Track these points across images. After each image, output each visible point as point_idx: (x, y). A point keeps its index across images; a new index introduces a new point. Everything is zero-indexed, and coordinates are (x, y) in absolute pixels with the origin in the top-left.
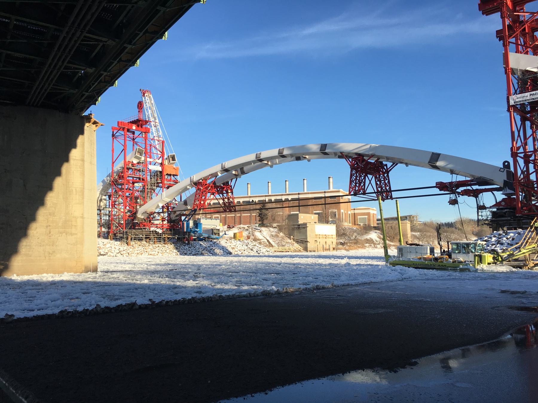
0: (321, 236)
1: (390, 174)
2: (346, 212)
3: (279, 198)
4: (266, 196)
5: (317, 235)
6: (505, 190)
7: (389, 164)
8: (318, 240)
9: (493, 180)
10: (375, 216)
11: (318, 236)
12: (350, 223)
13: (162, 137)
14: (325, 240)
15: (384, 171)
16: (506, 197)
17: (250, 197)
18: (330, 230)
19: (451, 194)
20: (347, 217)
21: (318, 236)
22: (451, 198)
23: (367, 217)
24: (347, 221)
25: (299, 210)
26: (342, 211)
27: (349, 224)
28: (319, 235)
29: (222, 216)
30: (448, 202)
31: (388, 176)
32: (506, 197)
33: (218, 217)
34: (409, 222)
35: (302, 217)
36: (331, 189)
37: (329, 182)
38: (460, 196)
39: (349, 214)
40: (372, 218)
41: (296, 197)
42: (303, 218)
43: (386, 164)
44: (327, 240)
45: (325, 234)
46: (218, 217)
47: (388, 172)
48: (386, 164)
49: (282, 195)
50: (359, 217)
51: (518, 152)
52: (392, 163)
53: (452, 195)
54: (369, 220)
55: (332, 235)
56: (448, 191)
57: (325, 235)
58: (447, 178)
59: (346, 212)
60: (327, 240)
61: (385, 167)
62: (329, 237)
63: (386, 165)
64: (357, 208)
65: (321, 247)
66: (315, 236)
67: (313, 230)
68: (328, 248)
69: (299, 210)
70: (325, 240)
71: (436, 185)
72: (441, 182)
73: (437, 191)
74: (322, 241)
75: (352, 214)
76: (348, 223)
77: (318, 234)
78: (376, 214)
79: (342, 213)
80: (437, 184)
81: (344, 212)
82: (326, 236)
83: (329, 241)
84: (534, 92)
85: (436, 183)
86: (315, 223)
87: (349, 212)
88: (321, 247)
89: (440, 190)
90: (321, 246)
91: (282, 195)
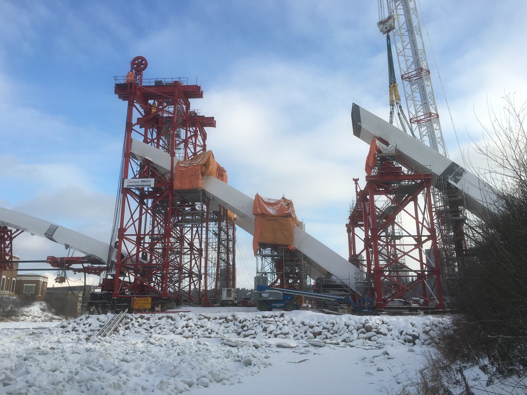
1: (14, 241)
6: (110, 272)
7: (14, 230)
9: (102, 259)
10: (45, 284)
15: (6, 236)
16: (112, 278)
19: (60, 270)
22: (59, 275)
23: (35, 285)
24: (9, 288)
26: (4, 277)
27: (11, 292)
30: (55, 280)
31: (11, 243)
32: (112, 278)
38: (77, 273)
39: (14, 281)
43: (12, 230)
47: (11, 239)
48: (12, 230)
50: (25, 285)
51: (125, 234)
52: (16, 230)
53: (61, 271)
56: (58, 267)
58: (61, 252)
59: (9, 278)
61: (9, 233)
63: (11, 231)
71: (47, 259)
72: (53, 257)
73: (49, 266)
76: (10, 291)
79: (4, 279)
80: (48, 259)
84: (145, 179)
85: (48, 257)
87: (14, 279)
89: (52, 266)
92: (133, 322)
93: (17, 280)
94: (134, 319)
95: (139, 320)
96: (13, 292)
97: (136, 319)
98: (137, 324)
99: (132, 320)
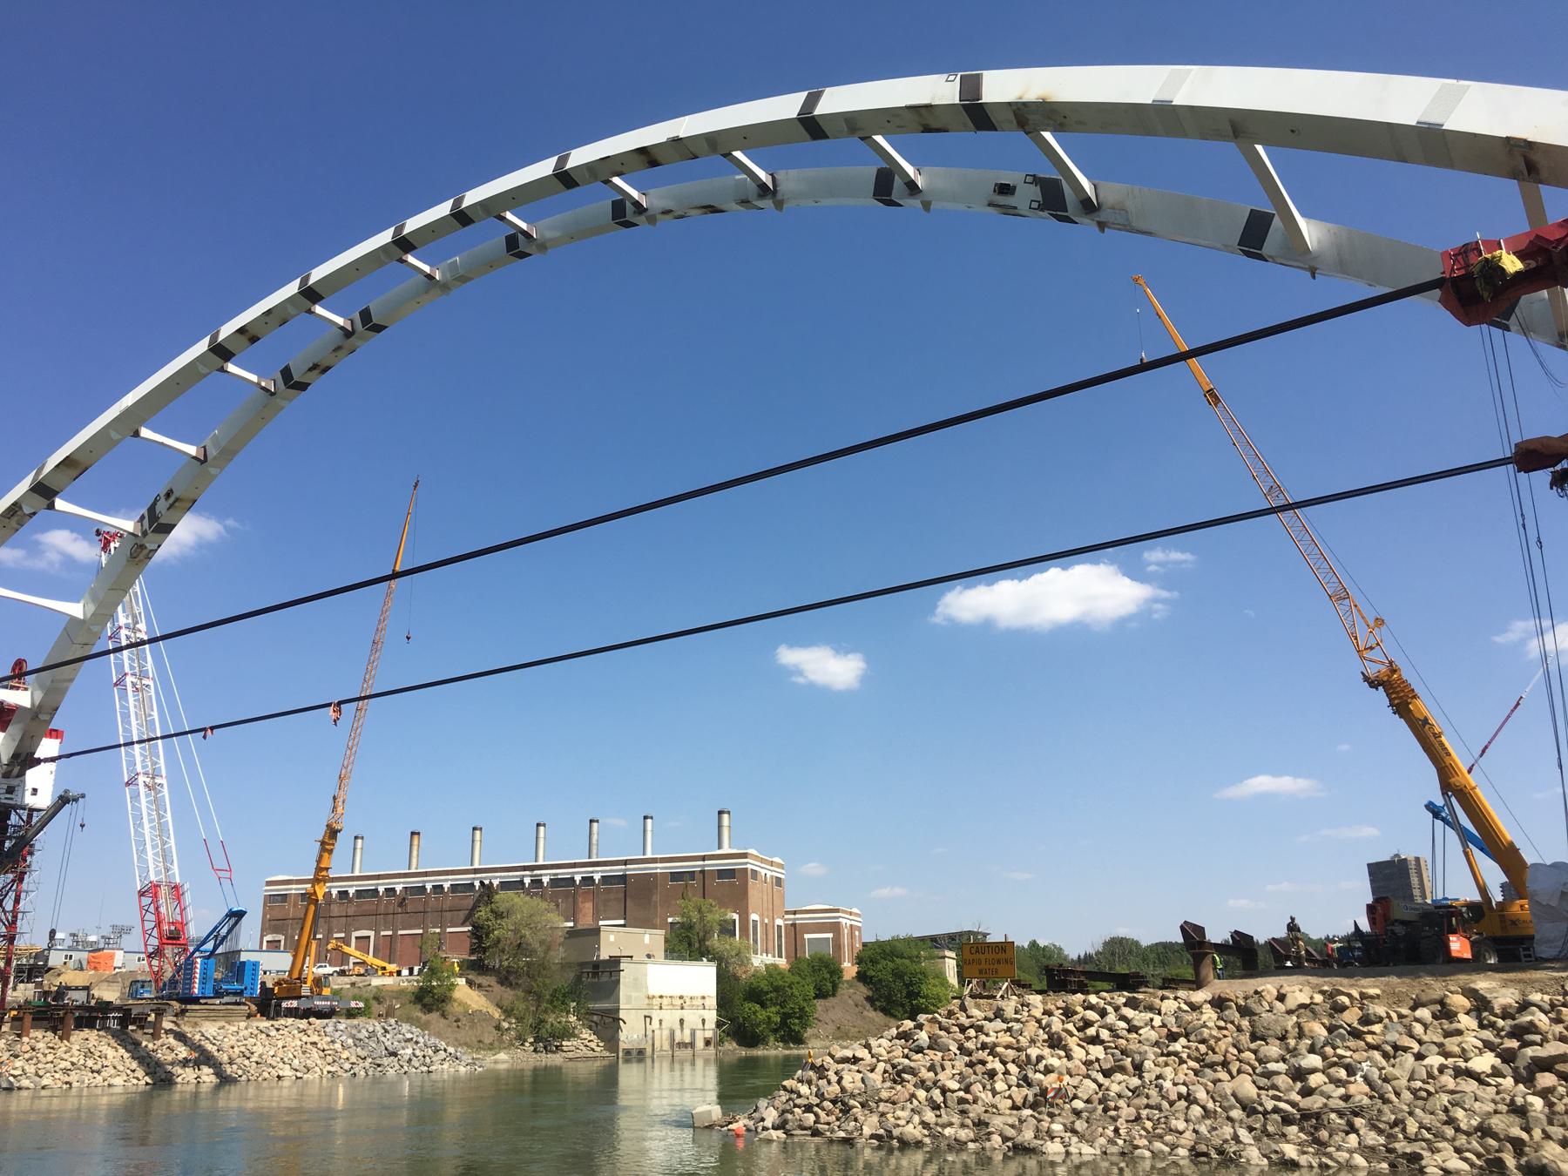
0: (665, 1002)
2: (766, 921)
3: (563, 873)
4: (525, 868)
5: (654, 997)
8: (656, 1015)
10: (857, 933)
11: (656, 1002)
12: (780, 956)
13: (151, 676)
14: (678, 1014)
17: (476, 871)
18: (700, 979)
20: (770, 937)
21: (656, 1002)
23: (830, 935)
24: (770, 947)
25: (625, 914)
26: (754, 917)
27: (777, 958)
28: (661, 997)
29: (383, 933)
33: (369, 937)
34: (953, 955)
35: (612, 938)
36: (726, 850)
37: (720, 826)
39: (779, 927)
40: (846, 941)
41: (617, 871)
42: (614, 939)
44: (686, 1014)
45: (679, 995)
46: (369, 937)
49: (574, 865)
54: (838, 946)
55: (704, 998)
57: (681, 997)
59: (766, 921)
60: (686, 1014)
62: (695, 1002)
64: (804, 908)
65: (664, 1038)
66: (647, 1001)
67: (639, 984)
68: (687, 1040)
69: (625, 914)
70: (678, 1014)
74: (671, 1017)
75: (786, 925)
77: (657, 994)
78: (859, 929)
81: (762, 921)
82: (683, 1002)
83: (692, 1018)
86: (649, 956)
87: (779, 922)
88: (664, 1038)
90: (666, 1033)
91: (574, 865)
92: (1111, 1018)
93: (786, 925)
94: (1110, 1009)
95: (1129, 1012)
96: (781, 957)
97: (1117, 1009)
98: (1123, 1025)
99: (1103, 1013)
